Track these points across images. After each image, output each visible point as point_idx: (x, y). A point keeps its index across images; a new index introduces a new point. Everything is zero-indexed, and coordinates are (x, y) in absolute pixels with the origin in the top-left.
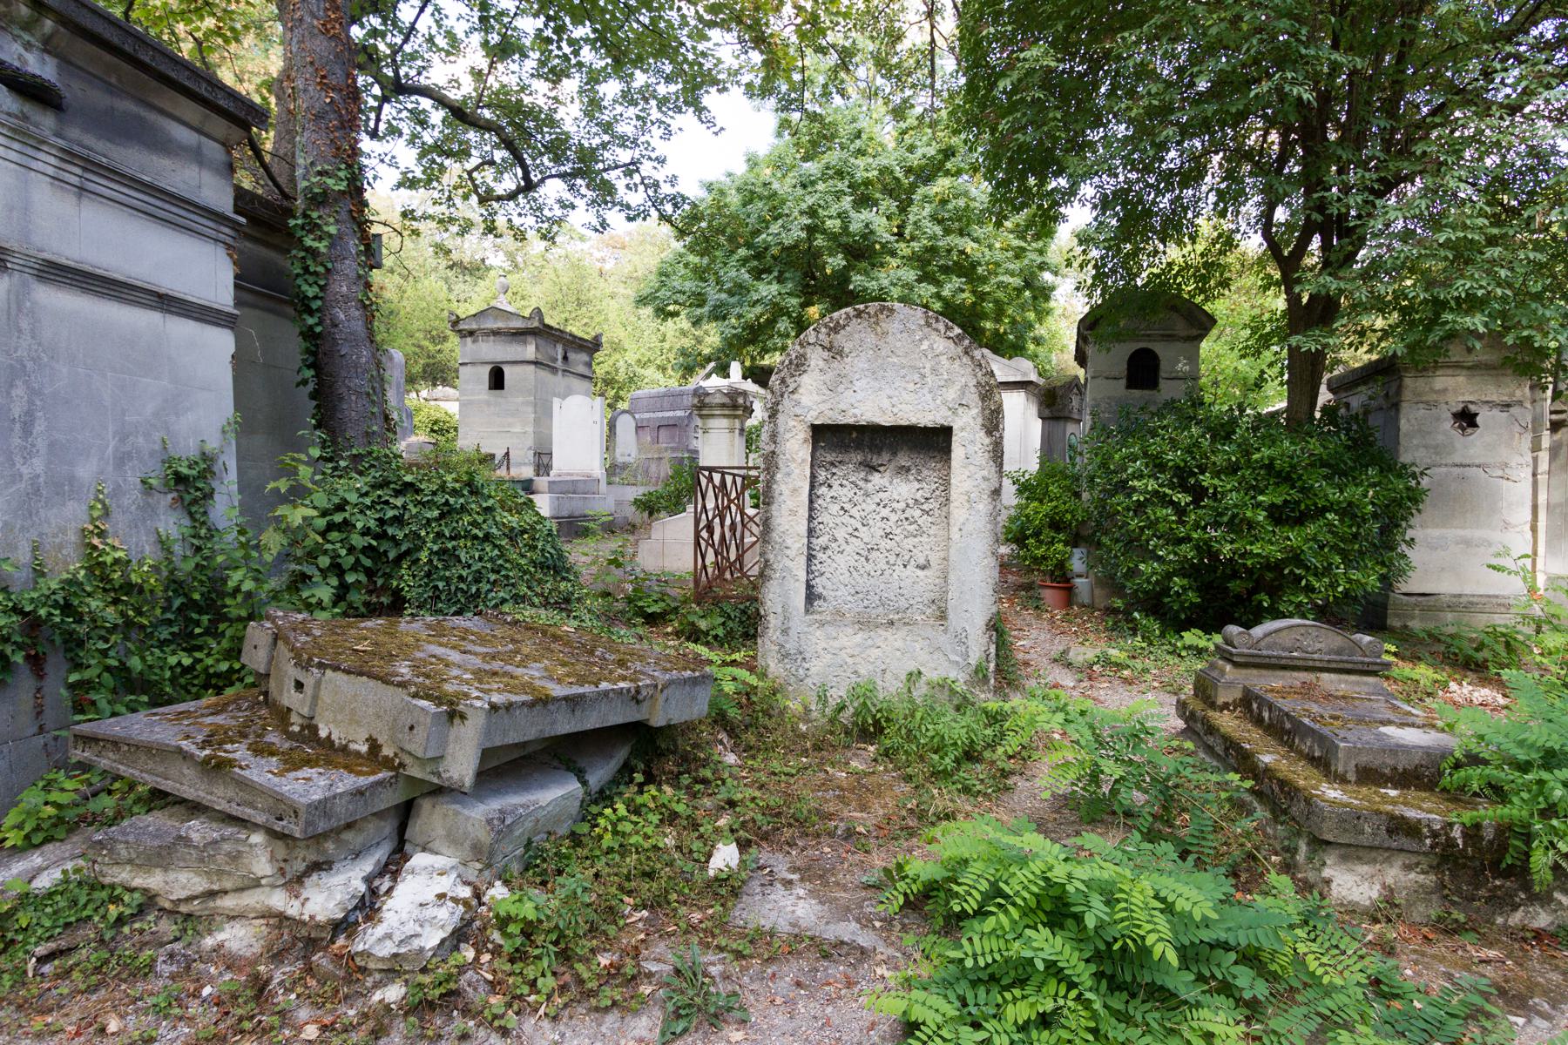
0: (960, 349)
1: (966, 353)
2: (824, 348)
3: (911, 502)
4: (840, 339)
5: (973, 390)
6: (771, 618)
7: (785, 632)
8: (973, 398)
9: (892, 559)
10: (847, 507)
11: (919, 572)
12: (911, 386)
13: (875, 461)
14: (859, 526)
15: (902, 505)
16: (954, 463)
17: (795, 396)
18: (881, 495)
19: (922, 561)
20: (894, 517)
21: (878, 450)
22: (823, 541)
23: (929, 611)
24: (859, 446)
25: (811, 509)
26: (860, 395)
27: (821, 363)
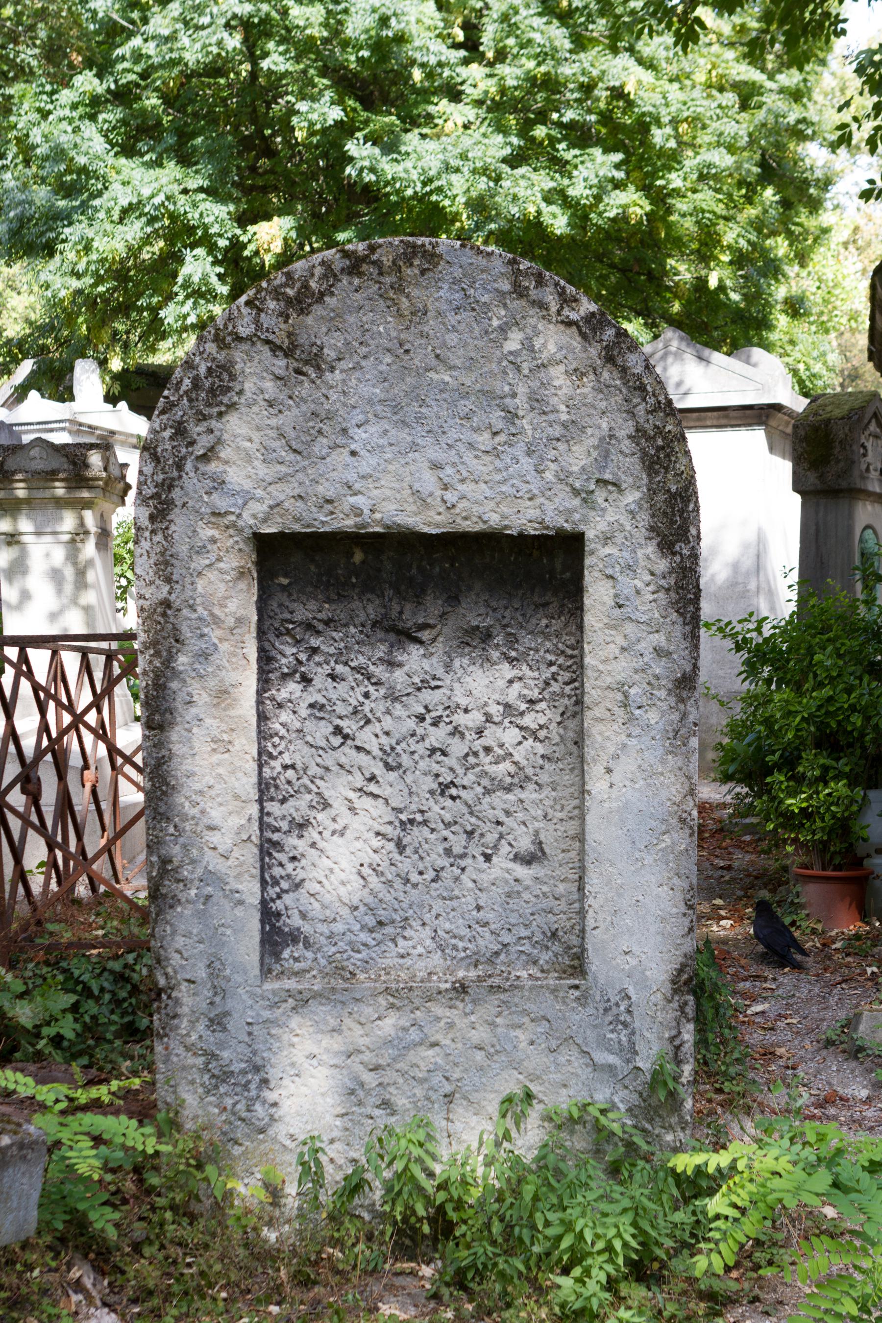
0: (594, 351)
1: (610, 359)
2: (275, 348)
3: (495, 710)
4: (313, 325)
5: (627, 445)
6: (183, 992)
7: (217, 1023)
8: (627, 464)
9: (458, 843)
10: (349, 726)
11: (521, 871)
12: (484, 440)
13: (410, 618)
14: (378, 769)
15: (475, 718)
16: (590, 619)
17: (213, 467)
18: (427, 696)
19: (525, 844)
20: (458, 748)
21: (414, 590)
22: (299, 806)
23: (545, 957)
24: (369, 585)
25: (263, 735)
26: (367, 463)
27: (269, 385)
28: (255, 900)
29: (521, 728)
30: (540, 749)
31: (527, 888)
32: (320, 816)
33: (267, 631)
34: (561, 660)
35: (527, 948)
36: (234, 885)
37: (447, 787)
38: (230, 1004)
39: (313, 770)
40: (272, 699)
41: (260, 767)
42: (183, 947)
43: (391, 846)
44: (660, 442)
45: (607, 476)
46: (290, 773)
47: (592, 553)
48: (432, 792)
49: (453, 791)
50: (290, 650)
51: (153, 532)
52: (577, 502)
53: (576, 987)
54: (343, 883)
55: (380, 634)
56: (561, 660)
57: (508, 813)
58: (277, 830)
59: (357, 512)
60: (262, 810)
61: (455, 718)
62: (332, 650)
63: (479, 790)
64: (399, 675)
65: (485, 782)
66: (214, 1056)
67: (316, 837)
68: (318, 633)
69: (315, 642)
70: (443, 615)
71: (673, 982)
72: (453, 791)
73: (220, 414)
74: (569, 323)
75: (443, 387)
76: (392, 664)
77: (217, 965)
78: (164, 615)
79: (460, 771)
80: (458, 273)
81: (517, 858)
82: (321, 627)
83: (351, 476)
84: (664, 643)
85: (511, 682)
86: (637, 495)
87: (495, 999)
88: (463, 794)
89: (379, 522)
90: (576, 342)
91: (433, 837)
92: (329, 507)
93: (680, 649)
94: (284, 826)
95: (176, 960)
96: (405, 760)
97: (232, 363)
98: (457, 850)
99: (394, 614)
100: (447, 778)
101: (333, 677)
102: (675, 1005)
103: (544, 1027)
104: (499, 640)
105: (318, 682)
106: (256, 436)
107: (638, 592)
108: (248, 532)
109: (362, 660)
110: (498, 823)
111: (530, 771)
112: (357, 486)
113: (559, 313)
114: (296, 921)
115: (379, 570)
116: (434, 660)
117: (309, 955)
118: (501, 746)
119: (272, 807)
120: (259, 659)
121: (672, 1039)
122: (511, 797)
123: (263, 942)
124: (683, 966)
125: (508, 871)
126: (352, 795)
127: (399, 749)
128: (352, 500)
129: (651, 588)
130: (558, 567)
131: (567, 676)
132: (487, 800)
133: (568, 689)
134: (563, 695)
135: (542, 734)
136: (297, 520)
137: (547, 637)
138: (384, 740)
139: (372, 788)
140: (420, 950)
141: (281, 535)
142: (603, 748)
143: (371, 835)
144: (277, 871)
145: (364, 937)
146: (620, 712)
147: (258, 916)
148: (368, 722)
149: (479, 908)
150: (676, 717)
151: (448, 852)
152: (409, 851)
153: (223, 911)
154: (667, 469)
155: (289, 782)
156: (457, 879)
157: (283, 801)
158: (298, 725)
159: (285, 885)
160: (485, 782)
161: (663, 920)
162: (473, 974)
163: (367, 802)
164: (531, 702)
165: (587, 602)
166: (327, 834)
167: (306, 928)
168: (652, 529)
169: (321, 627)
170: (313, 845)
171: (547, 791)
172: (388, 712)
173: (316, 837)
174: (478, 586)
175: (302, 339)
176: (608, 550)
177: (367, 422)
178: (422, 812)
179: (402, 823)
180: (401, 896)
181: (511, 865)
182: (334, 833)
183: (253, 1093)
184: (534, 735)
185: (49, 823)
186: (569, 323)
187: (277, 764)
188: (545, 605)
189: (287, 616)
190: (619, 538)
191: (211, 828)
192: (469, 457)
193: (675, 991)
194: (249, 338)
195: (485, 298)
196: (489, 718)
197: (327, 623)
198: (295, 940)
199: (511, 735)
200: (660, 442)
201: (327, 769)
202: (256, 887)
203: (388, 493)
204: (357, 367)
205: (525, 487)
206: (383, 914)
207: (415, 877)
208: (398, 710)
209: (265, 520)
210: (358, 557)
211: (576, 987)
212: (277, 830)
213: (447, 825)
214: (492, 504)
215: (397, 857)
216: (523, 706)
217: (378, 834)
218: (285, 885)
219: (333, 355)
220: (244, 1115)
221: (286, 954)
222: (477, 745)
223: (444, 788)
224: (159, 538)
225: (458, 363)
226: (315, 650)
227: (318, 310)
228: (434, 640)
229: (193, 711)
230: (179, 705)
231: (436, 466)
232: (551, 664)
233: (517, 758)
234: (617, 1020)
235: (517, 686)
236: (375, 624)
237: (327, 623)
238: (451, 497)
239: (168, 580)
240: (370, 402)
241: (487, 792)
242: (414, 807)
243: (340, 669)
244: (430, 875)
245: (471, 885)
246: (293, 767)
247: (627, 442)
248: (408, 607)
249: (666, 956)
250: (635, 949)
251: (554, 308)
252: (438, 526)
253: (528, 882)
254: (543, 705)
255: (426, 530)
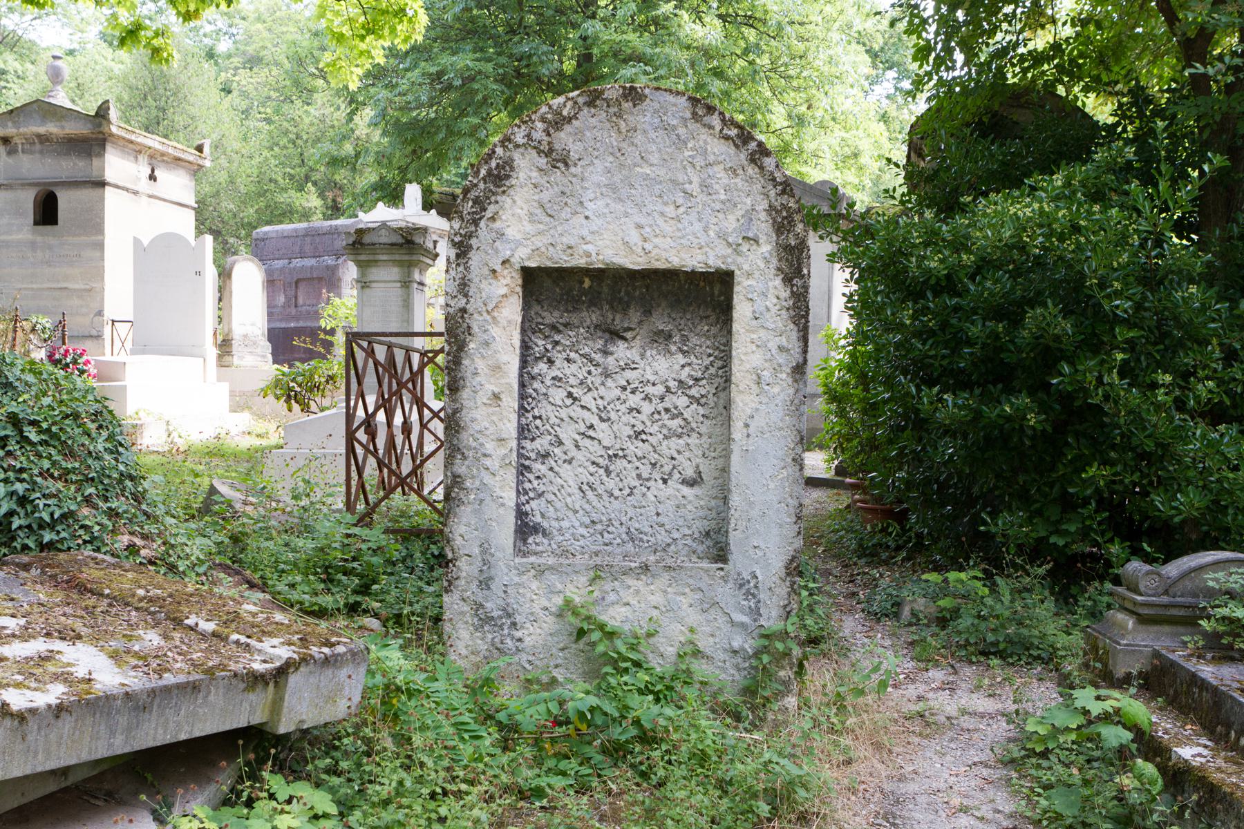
0: (743, 156)
1: (753, 161)
2: (540, 152)
3: (672, 384)
4: (564, 139)
5: (763, 216)
6: (462, 563)
7: (485, 584)
8: (763, 227)
9: (645, 471)
10: (576, 392)
11: (686, 490)
12: (670, 210)
13: (619, 322)
14: (595, 421)
15: (660, 389)
16: (736, 326)
17: (498, 225)
18: (628, 374)
19: (690, 473)
20: (647, 408)
21: (620, 304)
22: (542, 444)
23: (700, 548)
24: (594, 301)
25: (523, 396)
26: (596, 223)
27: (535, 174)
28: (512, 503)
29: (689, 397)
30: (701, 411)
31: (690, 502)
32: (556, 450)
33: (528, 328)
34: (716, 353)
35: (689, 542)
36: (498, 492)
37: (640, 433)
38: (493, 572)
39: (553, 420)
40: (529, 373)
41: (519, 416)
42: (463, 533)
43: (602, 471)
44: (785, 214)
45: (750, 235)
46: (538, 422)
47: (739, 284)
48: (629, 437)
49: (644, 437)
50: (541, 343)
51: (458, 265)
52: (730, 251)
53: (722, 569)
54: (569, 495)
55: (599, 334)
56: (716, 353)
57: (679, 452)
58: (529, 458)
59: (588, 255)
60: (519, 444)
61: (646, 389)
62: (568, 343)
63: (661, 436)
64: (611, 359)
65: (665, 431)
66: (481, 606)
67: (553, 464)
68: (559, 332)
69: (557, 338)
70: (640, 322)
71: (787, 568)
72: (644, 437)
73: (504, 192)
74: (727, 138)
75: (646, 177)
76: (606, 353)
77: (486, 545)
78: (462, 317)
79: (649, 424)
80: (657, 106)
81: (684, 482)
82: (561, 328)
83: (585, 232)
84: (785, 344)
85: (683, 366)
86: (769, 248)
87: (666, 575)
88: (649, 438)
89: (603, 262)
90: (732, 150)
91: (629, 466)
92: (570, 251)
93: (796, 347)
94: (533, 456)
95: (458, 541)
96: (613, 415)
97: (512, 160)
98: (645, 475)
99: (609, 321)
100: (640, 427)
101: (568, 360)
102: (788, 583)
103: (699, 595)
104: (677, 339)
105: (558, 363)
106: (526, 207)
107: (768, 310)
108: (517, 266)
109: (587, 350)
110: (673, 458)
111: (694, 425)
112: (588, 239)
113: (721, 131)
114: (538, 519)
115: (600, 293)
116: (634, 350)
117: (545, 541)
118: (676, 408)
119: (527, 444)
120: (521, 347)
121: (785, 607)
122: (681, 442)
123: (516, 531)
124: (794, 557)
125: (678, 490)
126: (578, 437)
127: (609, 408)
128: (585, 247)
129: (778, 307)
130: (716, 292)
131: (720, 363)
132: (665, 443)
133: (720, 372)
134: (717, 376)
135: (703, 401)
136: (550, 259)
137: (708, 338)
138: (600, 402)
139: (591, 433)
140: (619, 541)
141: (539, 268)
142: (743, 411)
143: (589, 464)
144: (527, 486)
145: (582, 531)
146: (754, 387)
147: (514, 514)
148: (590, 390)
149: (658, 514)
150: (792, 391)
151: (639, 476)
152: (613, 475)
153: (490, 510)
154: (789, 231)
155: (537, 428)
156: (644, 495)
157: (533, 440)
158: (544, 391)
159: (531, 494)
160: (665, 431)
161: (781, 526)
162: (652, 558)
163: (587, 442)
164: (696, 380)
165: (735, 315)
166: (560, 462)
167: (545, 524)
168: (779, 269)
169: (561, 328)
170: (551, 469)
171: (705, 438)
172: (603, 384)
173: (553, 464)
174: (664, 304)
175: (557, 146)
176: (749, 282)
177: (596, 198)
178: (623, 450)
179: (609, 456)
180: (607, 505)
181: (680, 486)
182: (565, 461)
183: (506, 632)
184: (698, 402)
185: (381, 452)
186: (727, 138)
187: (530, 415)
188: (707, 317)
189: (540, 320)
190: (757, 274)
191: (485, 455)
192: (660, 221)
193: (788, 574)
194: (524, 145)
195: (674, 122)
196: (668, 390)
197: (566, 325)
198: (537, 532)
199: (682, 401)
200: (785, 214)
201: (562, 420)
202: (514, 494)
203: (608, 243)
204: (592, 164)
205: (697, 241)
206: (595, 517)
207: (616, 493)
208: (609, 382)
209: (529, 259)
210: (587, 283)
211: (722, 569)
212: (529, 458)
213: (639, 459)
214: (675, 251)
215: (605, 478)
216: (691, 383)
217: (593, 463)
218: (531, 494)
219: (577, 157)
220: (499, 646)
221: (530, 540)
222: (660, 407)
223: (638, 434)
224: (461, 269)
225: (655, 162)
226: (557, 343)
227: (567, 128)
228: (634, 338)
229: (478, 379)
230: (468, 375)
231: (639, 226)
232: (710, 355)
233: (686, 416)
234: (748, 593)
235: (687, 369)
236: (596, 327)
237: (566, 325)
238: (648, 246)
239: (466, 295)
240: (598, 185)
241: (666, 437)
242: (618, 446)
243: (573, 355)
244: (627, 491)
245: (653, 499)
246: (540, 417)
247: (764, 214)
248: (618, 317)
249: (782, 550)
250: (762, 546)
251: (718, 128)
252: (639, 264)
253: (691, 498)
254: (704, 382)
255: (631, 267)
